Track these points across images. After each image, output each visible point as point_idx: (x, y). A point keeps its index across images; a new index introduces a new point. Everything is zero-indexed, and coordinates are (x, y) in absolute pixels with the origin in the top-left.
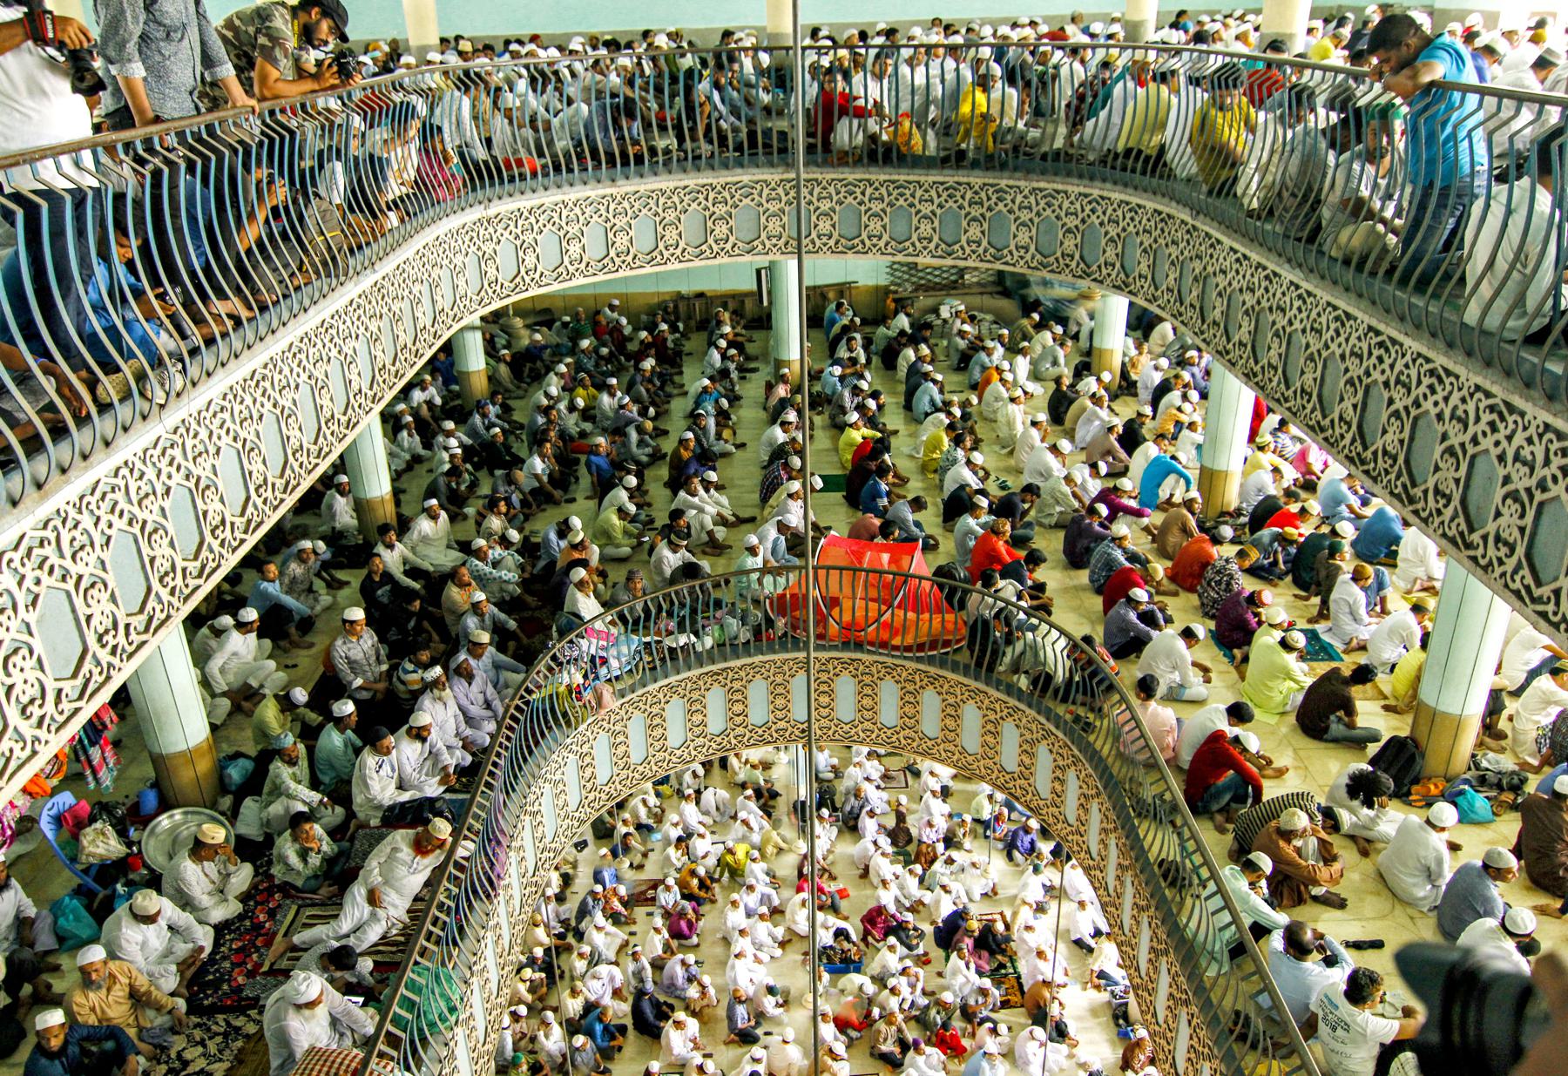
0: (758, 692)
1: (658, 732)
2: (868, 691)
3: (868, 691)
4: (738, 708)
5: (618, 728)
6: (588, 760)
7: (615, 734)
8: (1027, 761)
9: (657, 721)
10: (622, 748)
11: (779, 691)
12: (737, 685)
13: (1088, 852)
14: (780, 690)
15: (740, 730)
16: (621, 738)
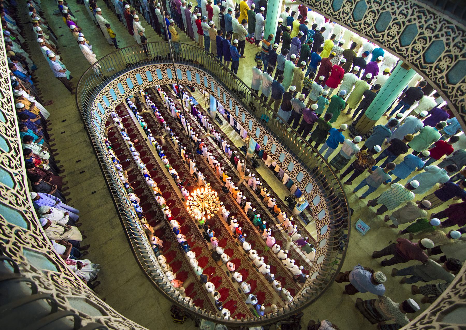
0: (128, 81)
1: (110, 98)
2: (154, 73)
3: (154, 73)
4: (126, 86)
5: (101, 100)
6: (98, 110)
7: (101, 102)
8: (194, 77)
9: (109, 95)
10: (104, 105)
11: (133, 79)
12: (123, 81)
13: (212, 91)
14: (134, 79)
15: (128, 91)
16: (103, 103)
